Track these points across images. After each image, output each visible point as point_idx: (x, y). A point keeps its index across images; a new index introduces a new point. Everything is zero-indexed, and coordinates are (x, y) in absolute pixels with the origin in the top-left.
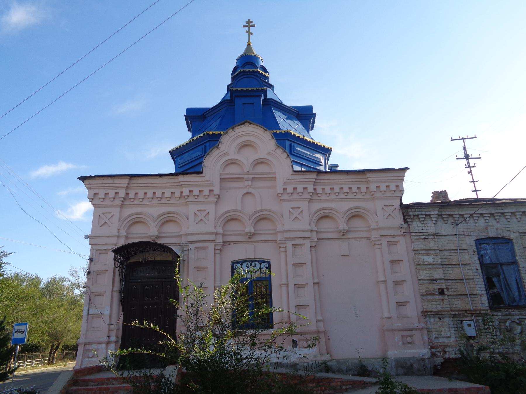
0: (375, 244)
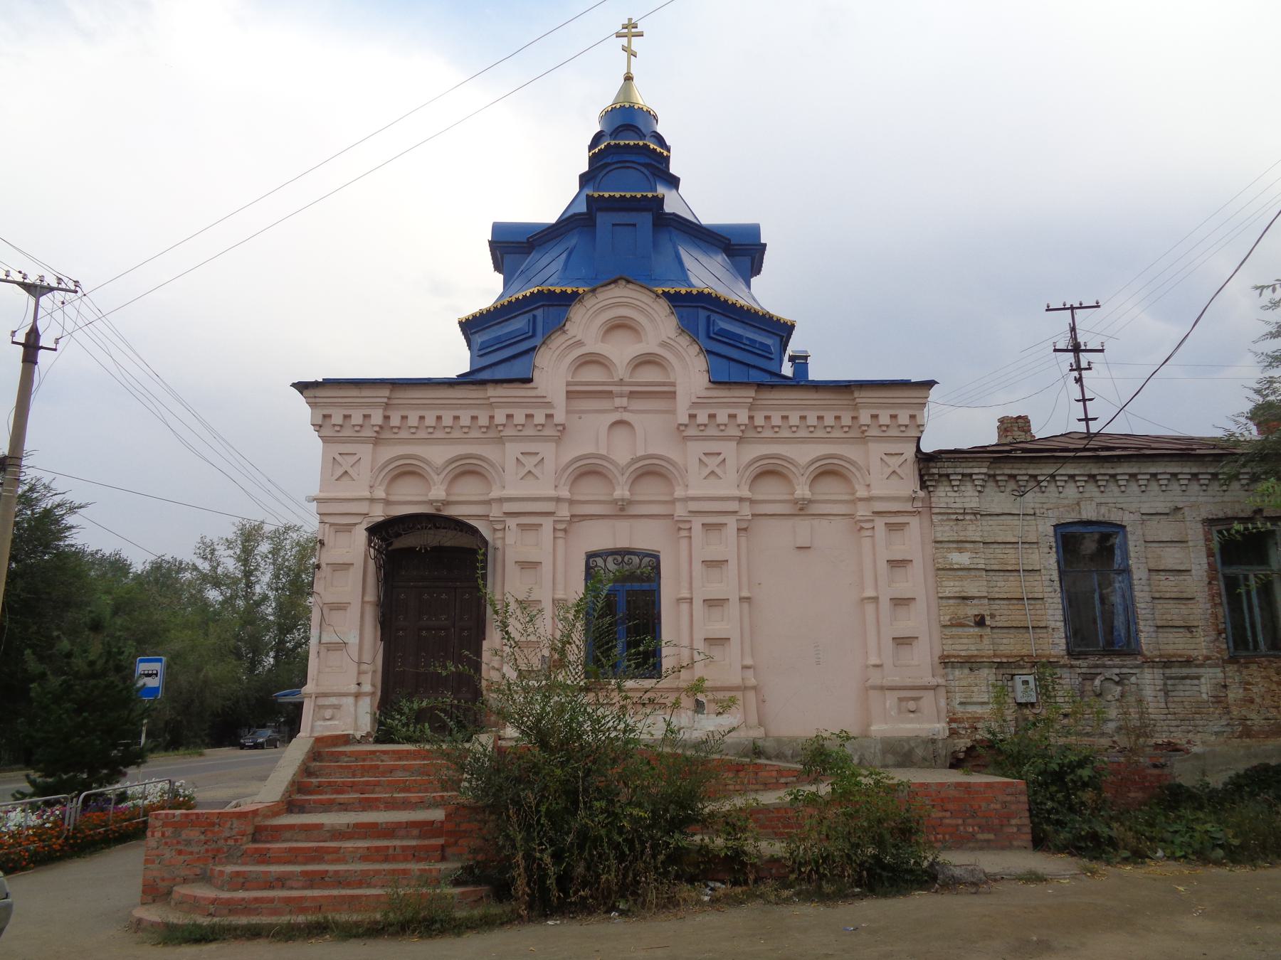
0: (862, 528)
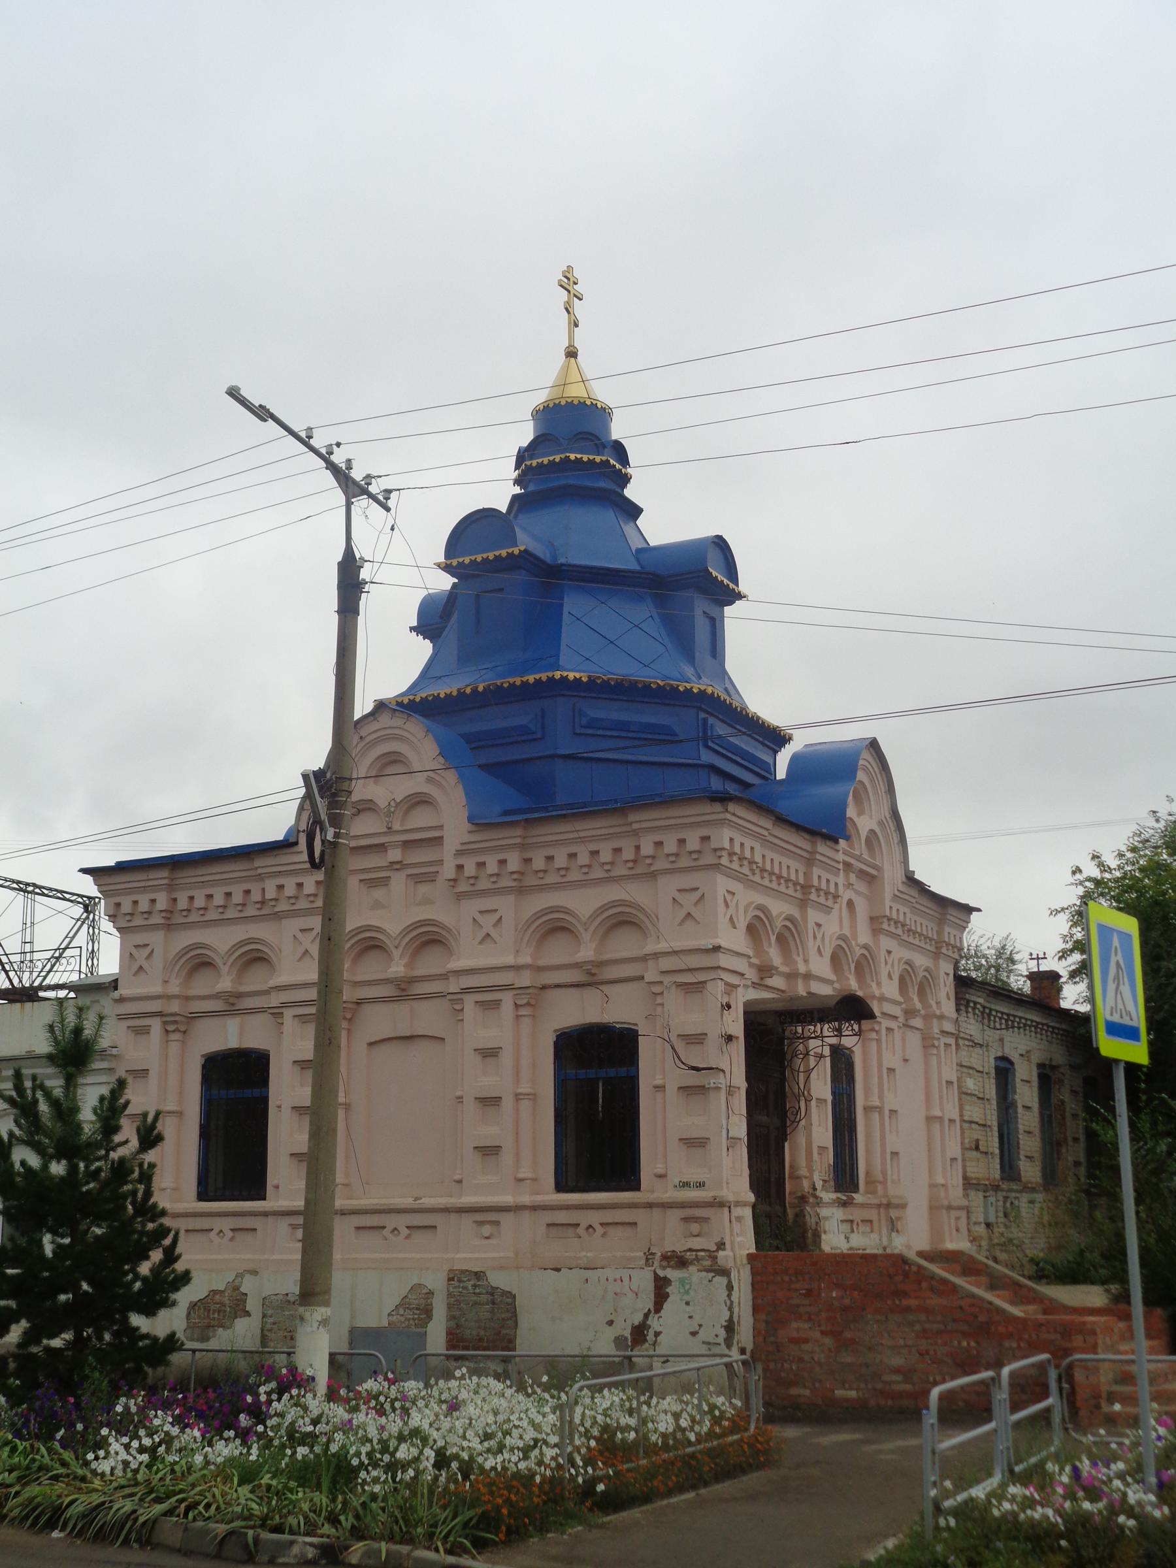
0: (933, 1046)
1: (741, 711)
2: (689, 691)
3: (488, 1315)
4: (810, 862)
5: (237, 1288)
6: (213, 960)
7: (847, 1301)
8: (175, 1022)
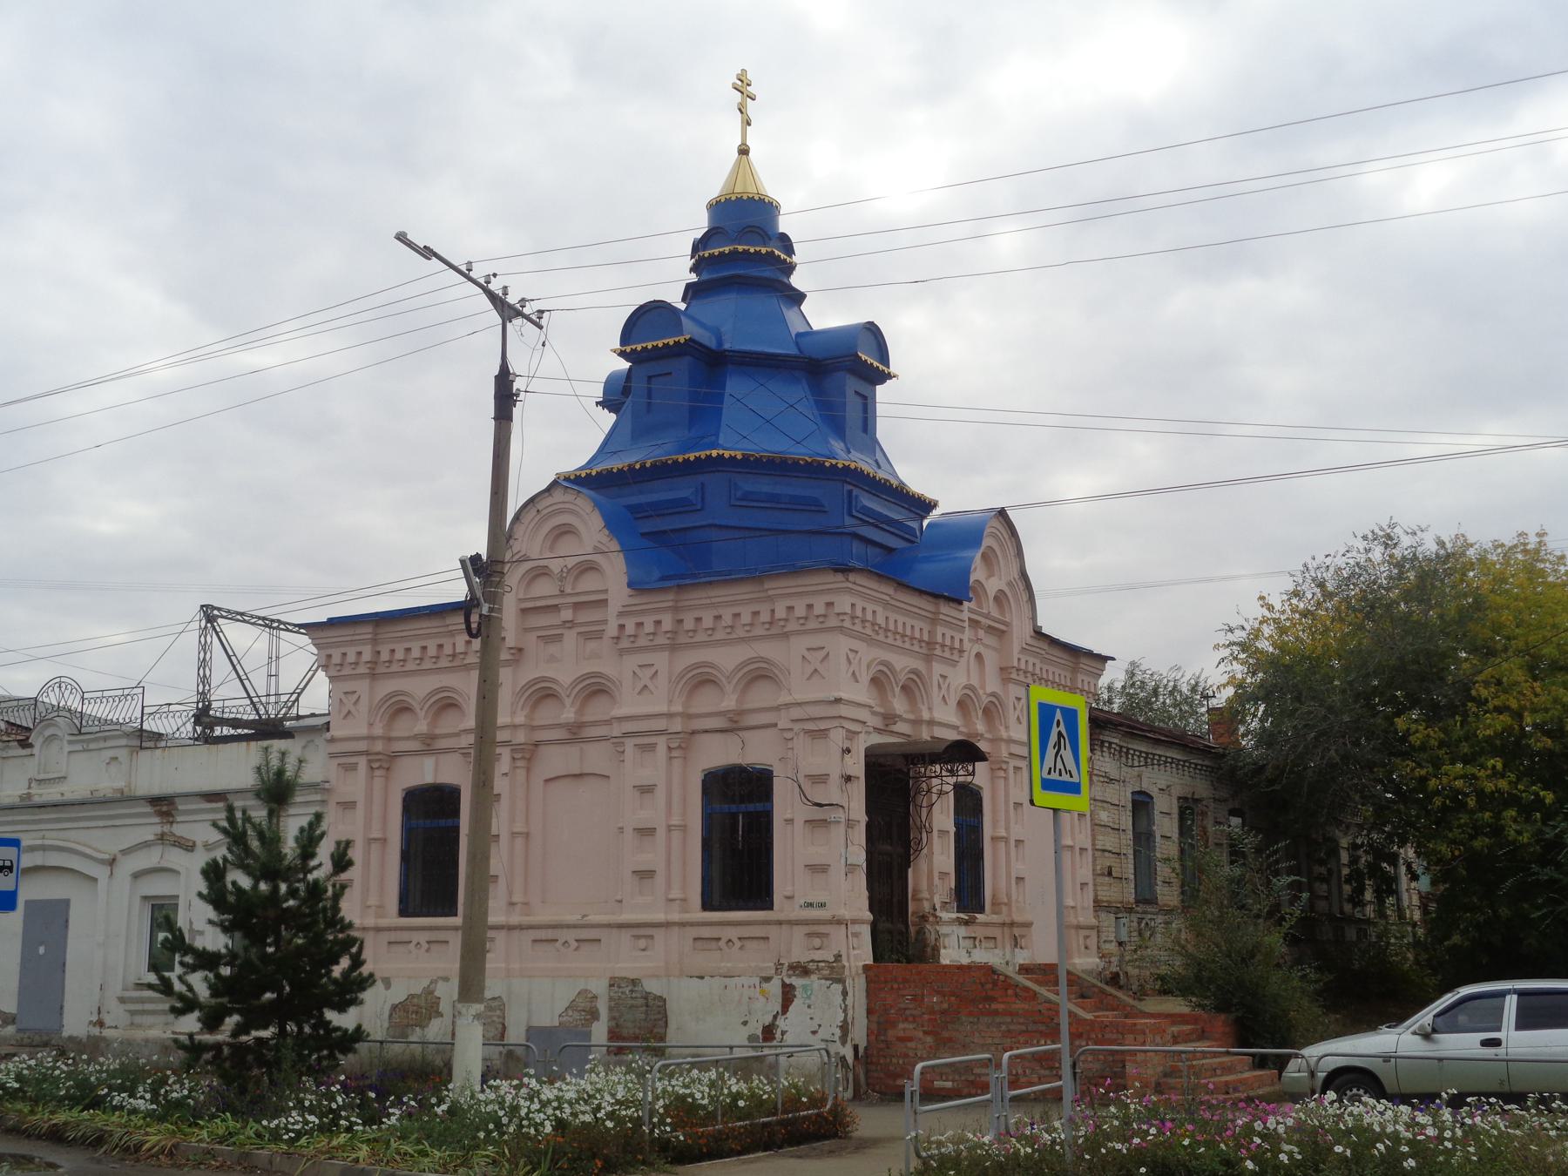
1: (885, 483)
2: (834, 467)
3: (643, 1016)
4: (934, 621)
5: (432, 993)
6: (409, 703)
7: (945, 1006)
8: (380, 760)
